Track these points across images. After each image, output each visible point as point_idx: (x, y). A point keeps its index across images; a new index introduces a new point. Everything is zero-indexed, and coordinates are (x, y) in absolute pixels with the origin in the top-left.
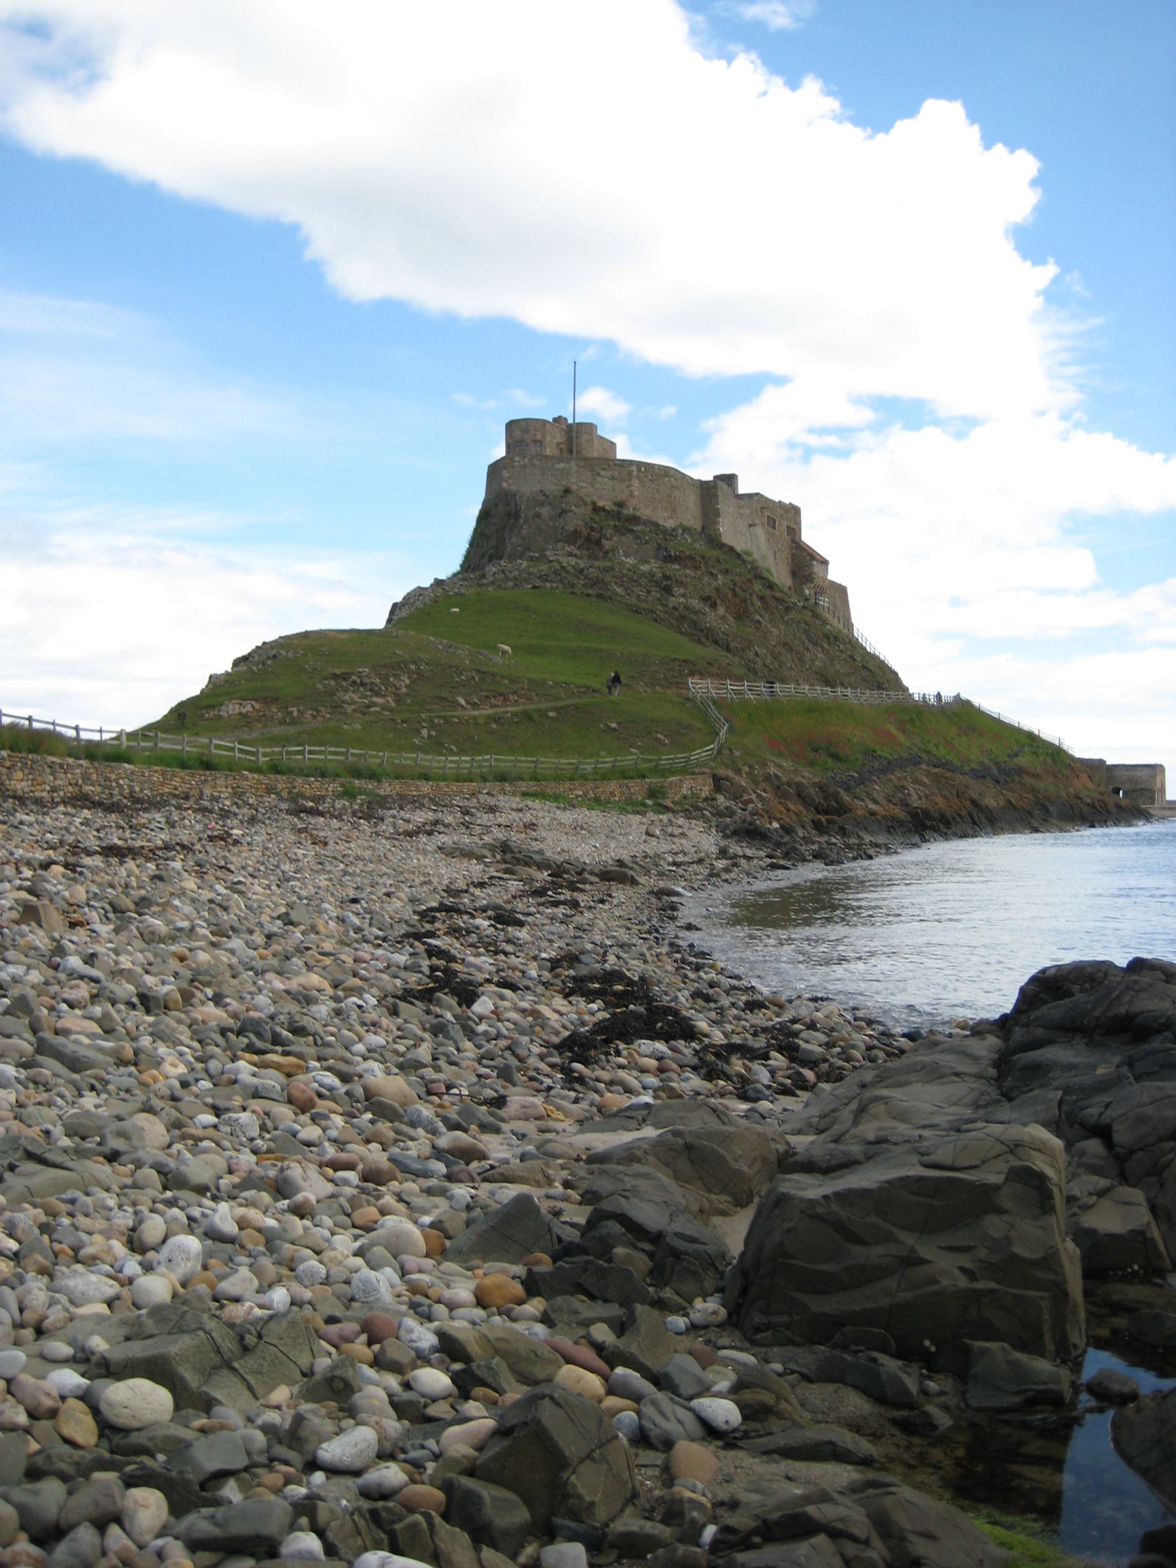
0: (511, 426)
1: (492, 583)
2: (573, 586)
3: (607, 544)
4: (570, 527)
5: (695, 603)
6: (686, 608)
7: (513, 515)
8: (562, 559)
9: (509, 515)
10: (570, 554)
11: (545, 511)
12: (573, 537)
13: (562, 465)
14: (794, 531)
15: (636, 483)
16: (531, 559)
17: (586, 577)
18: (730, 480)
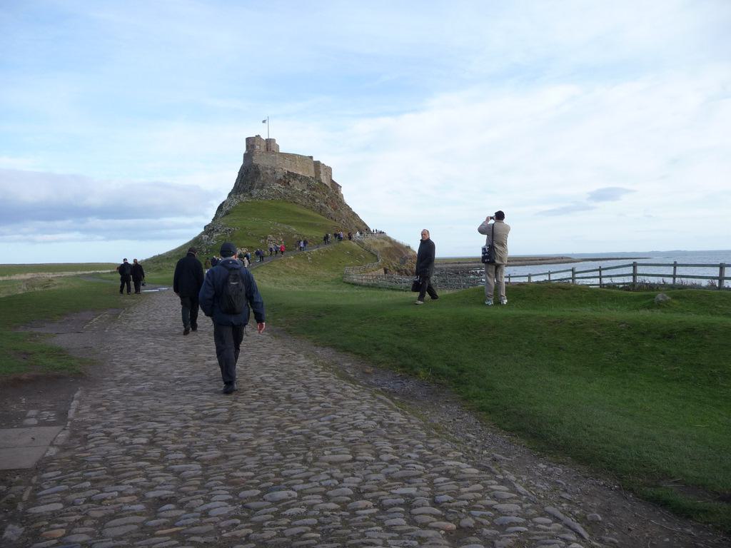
0: (248, 139)
5: (323, 205)
6: (321, 206)
7: (257, 173)
9: (256, 172)
11: (269, 171)
12: (280, 181)
14: (331, 176)
15: (298, 162)
18: (311, 157)
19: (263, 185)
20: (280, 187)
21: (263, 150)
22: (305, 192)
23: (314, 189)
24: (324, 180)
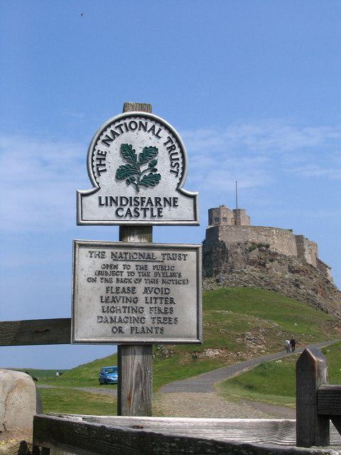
0: (210, 211)
1: (224, 285)
2: (260, 285)
3: (267, 265)
4: (251, 258)
5: (310, 292)
8: (251, 273)
10: (253, 271)
13: (244, 230)
16: (238, 273)
17: (265, 281)
19: (232, 268)
20: (253, 271)
21: (229, 223)
22: (287, 276)
23: (297, 272)
24: (309, 259)
